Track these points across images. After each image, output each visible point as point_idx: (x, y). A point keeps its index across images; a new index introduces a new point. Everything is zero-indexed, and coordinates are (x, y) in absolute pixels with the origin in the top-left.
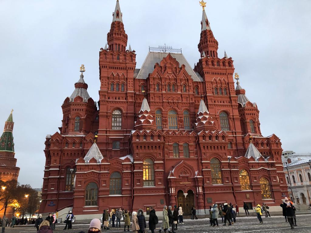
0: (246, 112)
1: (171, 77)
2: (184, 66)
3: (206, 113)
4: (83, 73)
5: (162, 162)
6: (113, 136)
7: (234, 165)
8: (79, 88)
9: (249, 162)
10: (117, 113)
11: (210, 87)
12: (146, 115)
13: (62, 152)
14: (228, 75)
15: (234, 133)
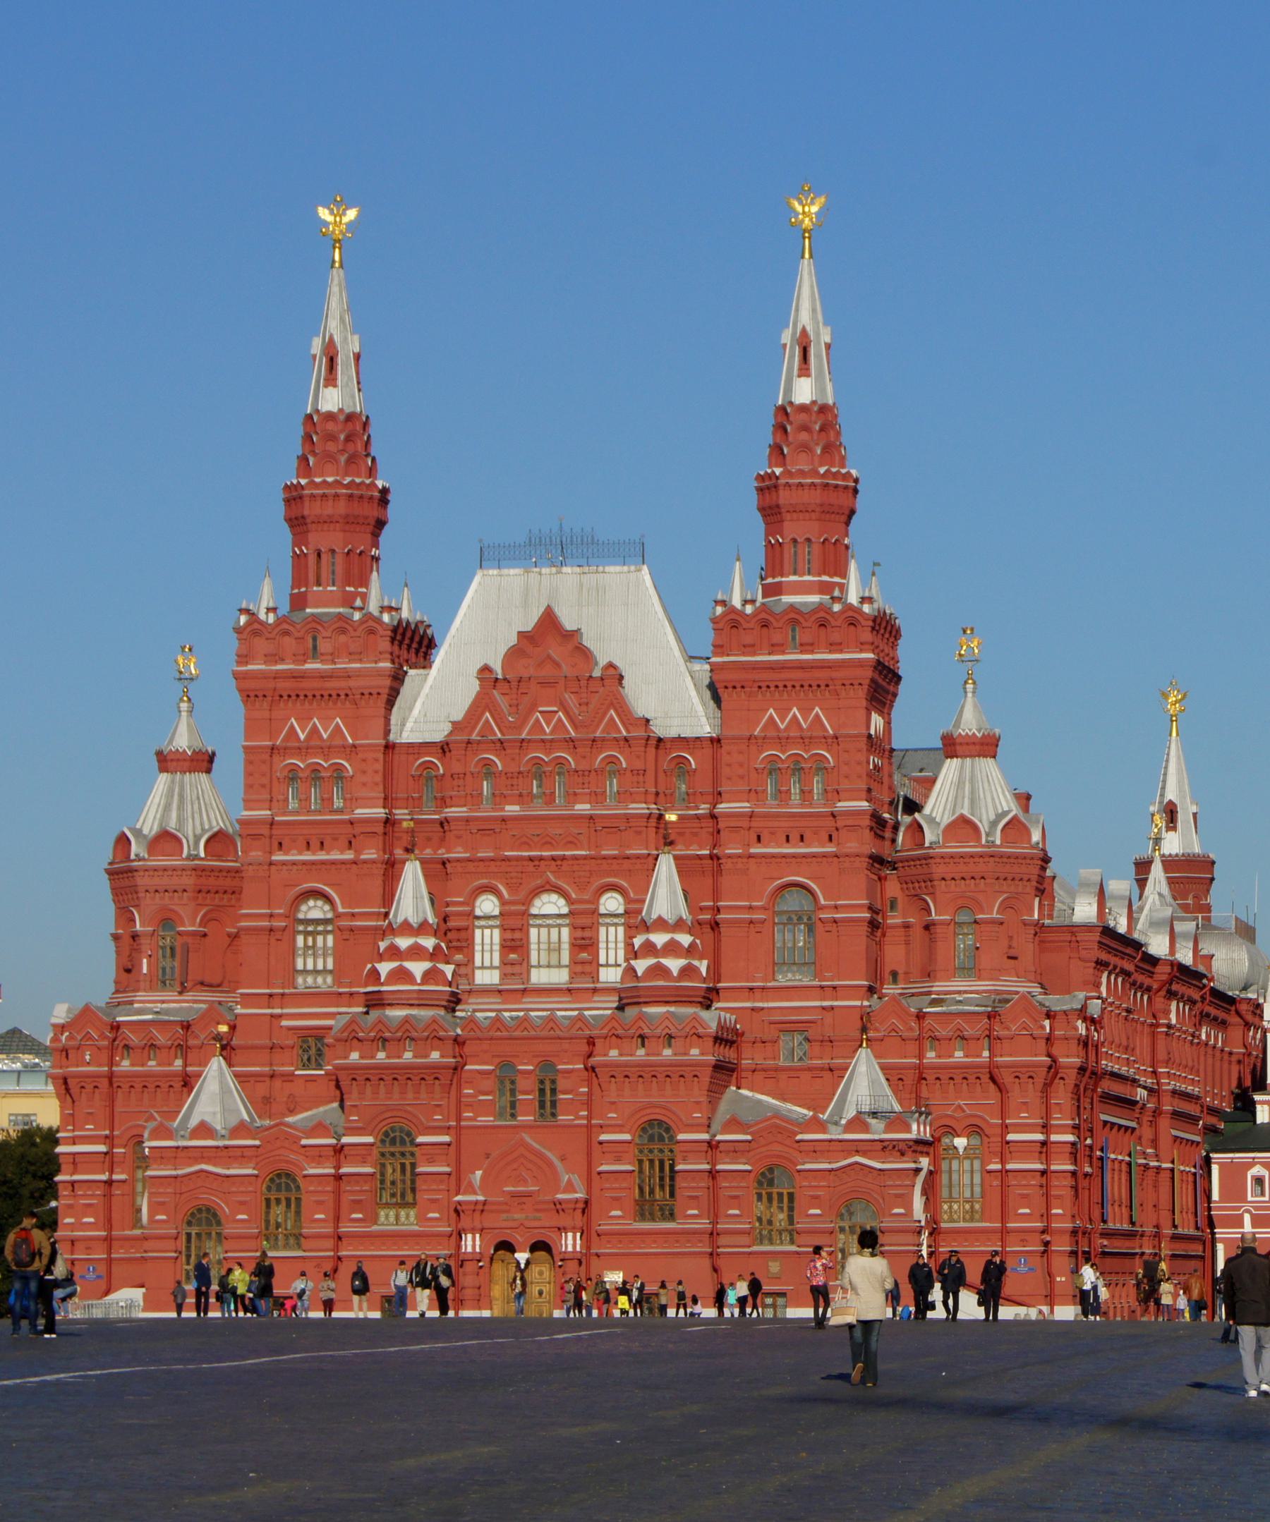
0: (938, 870)
1: (552, 733)
2: (611, 666)
3: (661, 924)
4: (192, 686)
5: (446, 1139)
6: (297, 1017)
7: (736, 1150)
8: (173, 772)
9: (799, 1137)
10: (314, 910)
11: (741, 765)
12: (404, 943)
13: (111, 1083)
14: (843, 694)
15: (829, 992)
